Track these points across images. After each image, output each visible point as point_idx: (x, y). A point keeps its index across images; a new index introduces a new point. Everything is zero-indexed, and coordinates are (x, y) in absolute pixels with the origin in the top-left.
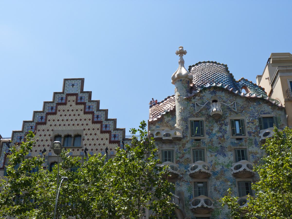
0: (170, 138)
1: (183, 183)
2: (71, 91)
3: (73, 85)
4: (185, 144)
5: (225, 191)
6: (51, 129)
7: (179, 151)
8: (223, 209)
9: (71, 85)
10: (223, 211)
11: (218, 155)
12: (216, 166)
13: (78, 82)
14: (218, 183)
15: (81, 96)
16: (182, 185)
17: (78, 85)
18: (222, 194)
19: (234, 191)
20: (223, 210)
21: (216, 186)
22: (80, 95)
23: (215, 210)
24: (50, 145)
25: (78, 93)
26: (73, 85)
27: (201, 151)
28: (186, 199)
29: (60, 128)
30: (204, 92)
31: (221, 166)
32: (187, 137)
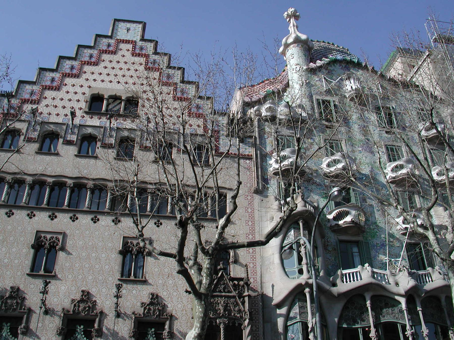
1: (314, 187)
2: (123, 36)
3: (128, 30)
6: (87, 85)
8: (379, 230)
13: (136, 26)
15: (140, 44)
17: (137, 30)
20: (379, 231)
22: (140, 43)
23: (368, 230)
24: (83, 108)
25: (135, 40)
26: (128, 30)
29: (102, 85)
30: (334, 65)
31: (369, 167)
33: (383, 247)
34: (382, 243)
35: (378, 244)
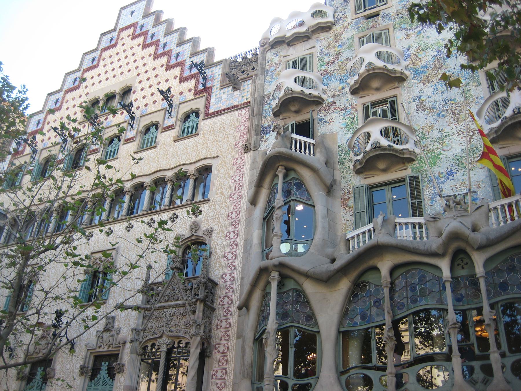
0: (303, 29)
1: (334, 115)
3: (133, 12)
4: (341, 34)
5: (449, 102)
7: (325, 51)
9: (131, 13)
10: (444, 153)
11: (426, 29)
12: (421, 55)
14: (428, 90)
16: (333, 120)
18: (441, 112)
19: (475, 97)
20: (445, 151)
21: (423, 98)
27: (381, 33)
28: (340, 149)
31: (434, 50)
32: (345, 17)
33: (451, 177)
34: (449, 170)
35: (442, 173)
